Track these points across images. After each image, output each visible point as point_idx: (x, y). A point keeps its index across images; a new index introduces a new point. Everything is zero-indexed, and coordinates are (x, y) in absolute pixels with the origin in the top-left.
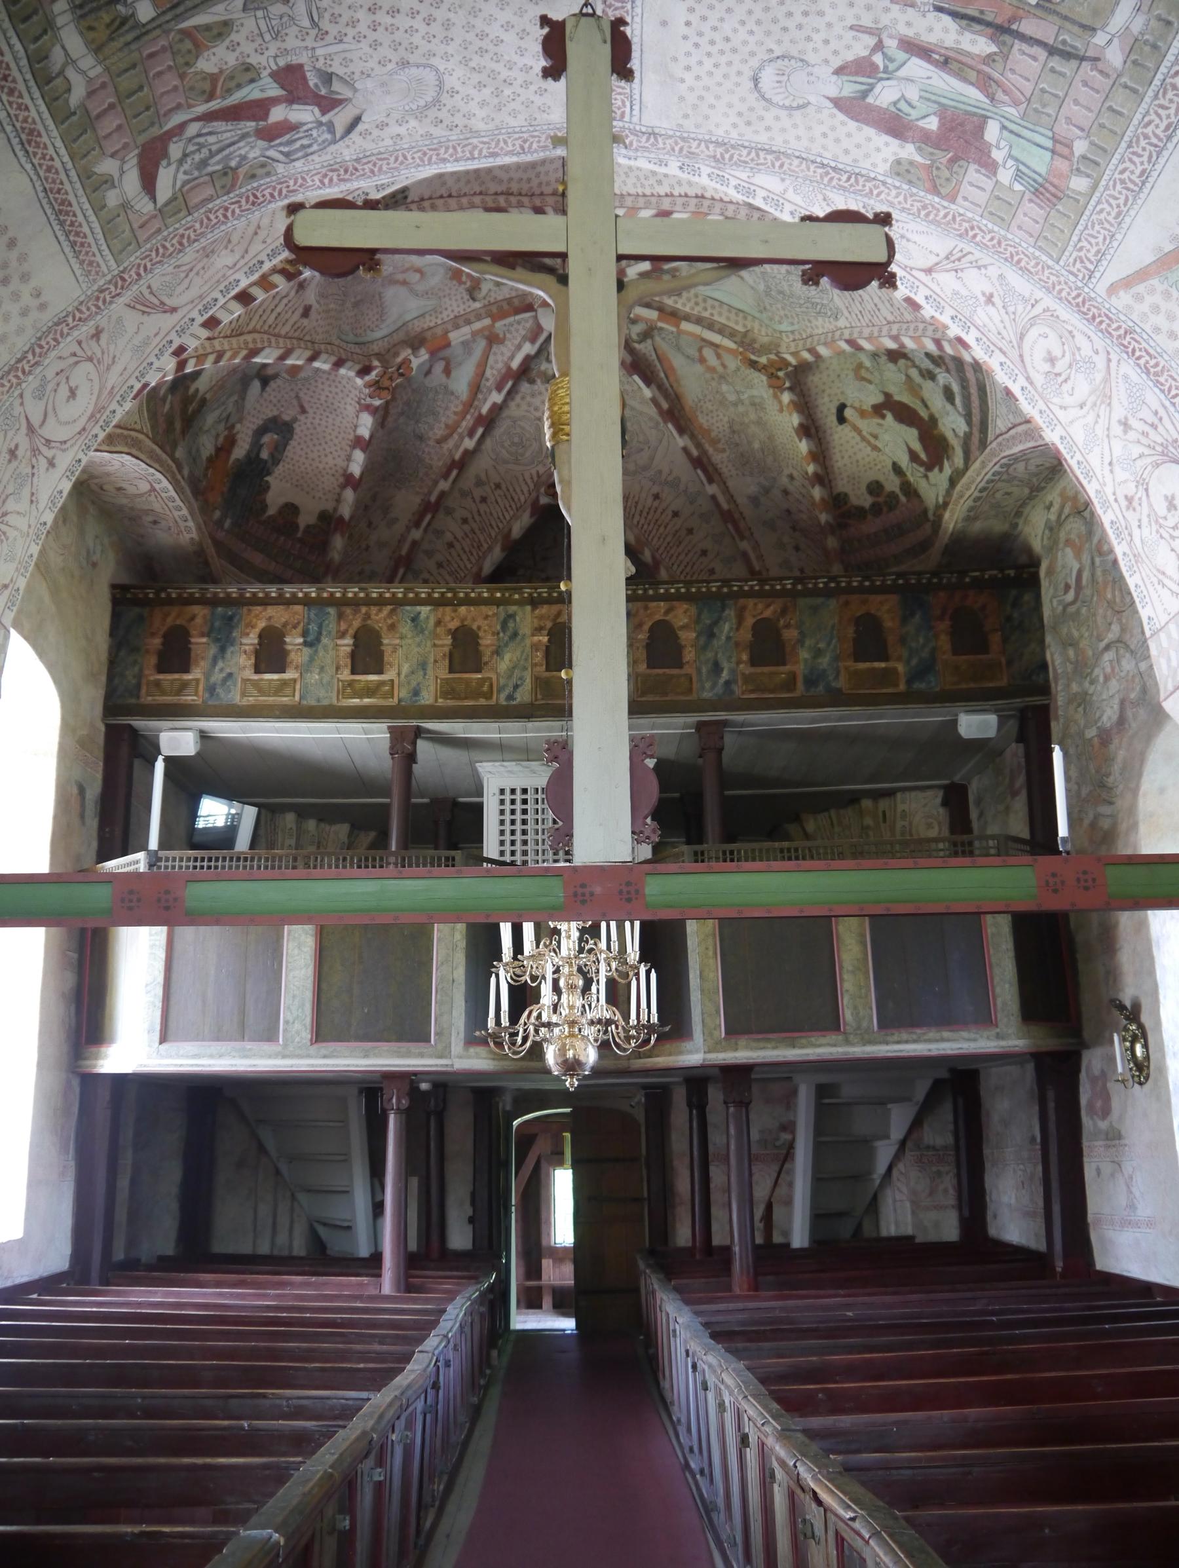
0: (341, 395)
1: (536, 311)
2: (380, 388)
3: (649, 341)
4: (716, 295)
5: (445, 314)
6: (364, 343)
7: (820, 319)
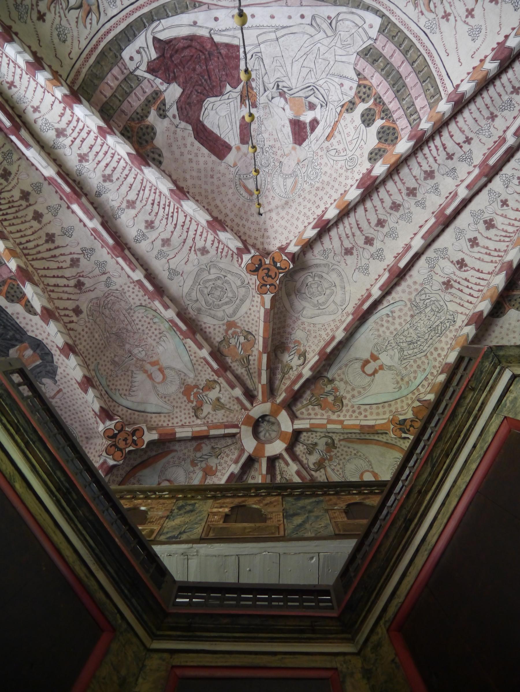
2: (114, 445)
4: (366, 401)
5: (175, 420)
6: (113, 401)
7: (443, 339)
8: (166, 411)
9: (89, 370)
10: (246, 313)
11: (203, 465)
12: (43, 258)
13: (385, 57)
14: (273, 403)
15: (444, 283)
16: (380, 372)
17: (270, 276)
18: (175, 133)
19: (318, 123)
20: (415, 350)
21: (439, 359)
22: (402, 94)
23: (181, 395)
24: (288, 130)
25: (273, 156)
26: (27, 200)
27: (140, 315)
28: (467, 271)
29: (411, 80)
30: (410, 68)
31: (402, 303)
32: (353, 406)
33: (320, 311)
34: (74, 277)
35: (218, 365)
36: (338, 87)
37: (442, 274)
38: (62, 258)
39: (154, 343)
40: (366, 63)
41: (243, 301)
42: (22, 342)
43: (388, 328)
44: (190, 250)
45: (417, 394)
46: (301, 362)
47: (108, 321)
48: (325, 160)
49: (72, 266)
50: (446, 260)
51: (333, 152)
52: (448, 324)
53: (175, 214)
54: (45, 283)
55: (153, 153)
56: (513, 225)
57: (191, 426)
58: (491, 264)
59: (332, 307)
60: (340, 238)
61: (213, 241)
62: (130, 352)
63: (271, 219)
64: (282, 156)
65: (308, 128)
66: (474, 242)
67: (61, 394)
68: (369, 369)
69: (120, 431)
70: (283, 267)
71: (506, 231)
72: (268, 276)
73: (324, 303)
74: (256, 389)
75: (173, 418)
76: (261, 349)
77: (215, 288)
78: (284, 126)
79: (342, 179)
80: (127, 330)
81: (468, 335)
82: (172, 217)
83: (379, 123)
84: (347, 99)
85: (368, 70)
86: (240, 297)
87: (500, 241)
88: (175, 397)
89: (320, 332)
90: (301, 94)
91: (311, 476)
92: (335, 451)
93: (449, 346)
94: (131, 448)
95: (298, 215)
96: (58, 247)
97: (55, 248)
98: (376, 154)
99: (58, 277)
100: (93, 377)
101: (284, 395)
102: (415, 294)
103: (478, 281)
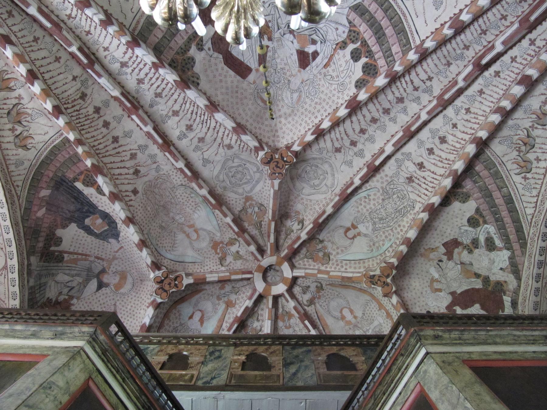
0: (140, 305)
1: (253, 274)
2: (162, 288)
3: (313, 306)
4: (347, 258)
5: (206, 268)
6: (161, 255)
7: (405, 219)
8: (199, 261)
9: (143, 234)
10: (260, 191)
11: (226, 299)
12: (110, 155)
13: (370, 12)
14: (278, 257)
15: (407, 178)
16: (358, 237)
17: (279, 167)
18: (210, 61)
19: (318, 54)
20: (385, 225)
21: (401, 233)
22: (382, 41)
23: (210, 249)
24: (295, 57)
25: (283, 75)
26: (99, 113)
27: (181, 192)
28: (425, 171)
29: (389, 31)
30: (388, 23)
31: (377, 190)
32: (337, 261)
33: (315, 191)
34: (133, 167)
35: (238, 228)
36: (334, 30)
37: (406, 172)
38: (124, 153)
39: (191, 212)
40: (356, 15)
41: (258, 182)
42: (94, 214)
43: (365, 207)
44: (219, 146)
45: (384, 256)
46: (300, 227)
47: (157, 197)
48: (322, 82)
49: (131, 159)
50: (410, 161)
51: (329, 77)
52: (409, 209)
53: (209, 121)
54: (112, 173)
55: (193, 77)
56: (460, 143)
57: (217, 272)
58: (442, 169)
59: (324, 189)
60: (332, 141)
61: (237, 140)
62: (173, 218)
63: (280, 122)
64: (290, 76)
65: (311, 57)
66: (431, 151)
67: (122, 249)
68: (350, 234)
69: (165, 278)
70: (289, 161)
71: (455, 147)
72: (277, 166)
73: (318, 185)
74: (266, 245)
75: (204, 266)
76: (270, 218)
77: (237, 172)
78: (292, 54)
79: (335, 98)
80: (171, 203)
81: (423, 219)
82: (206, 122)
83: (364, 60)
84: (341, 39)
85: (357, 21)
86: (256, 179)
87: (450, 153)
88: (206, 250)
89: (315, 206)
90: (306, 32)
91: (305, 310)
92: (323, 292)
93: (409, 225)
94: (174, 290)
95: (301, 122)
96: (121, 146)
97: (119, 147)
98: (361, 83)
99: (121, 168)
100: (146, 239)
101: (286, 251)
102: (386, 183)
103: (433, 180)
